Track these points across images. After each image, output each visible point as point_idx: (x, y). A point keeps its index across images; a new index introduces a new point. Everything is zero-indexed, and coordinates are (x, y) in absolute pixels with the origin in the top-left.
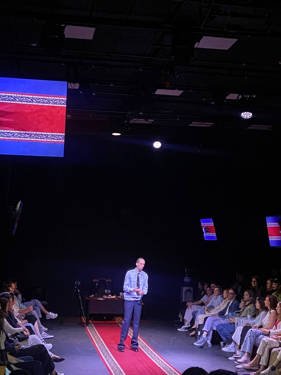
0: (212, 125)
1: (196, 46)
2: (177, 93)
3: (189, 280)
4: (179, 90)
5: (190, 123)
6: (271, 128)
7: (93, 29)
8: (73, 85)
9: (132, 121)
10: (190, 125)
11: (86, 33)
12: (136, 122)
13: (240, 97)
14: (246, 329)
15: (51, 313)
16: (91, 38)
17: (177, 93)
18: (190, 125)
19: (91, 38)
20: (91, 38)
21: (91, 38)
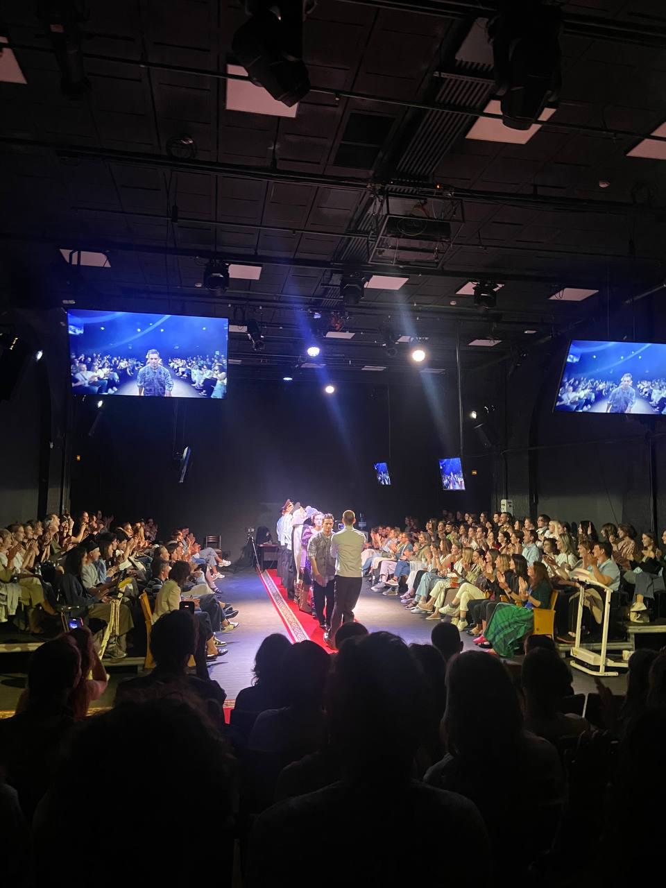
0: (385, 369)
1: (365, 286)
2: (348, 335)
3: (365, 525)
4: (350, 332)
5: (363, 367)
6: (444, 371)
7: (259, 269)
8: (240, 327)
9: (302, 367)
10: (363, 369)
11: (252, 273)
12: (308, 367)
13: (412, 339)
14: (420, 574)
15: (224, 561)
16: (257, 278)
17: (348, 335)
18: (363, 369)
19: (257, 278)
20: (257, 278)
21: (257, 278)
